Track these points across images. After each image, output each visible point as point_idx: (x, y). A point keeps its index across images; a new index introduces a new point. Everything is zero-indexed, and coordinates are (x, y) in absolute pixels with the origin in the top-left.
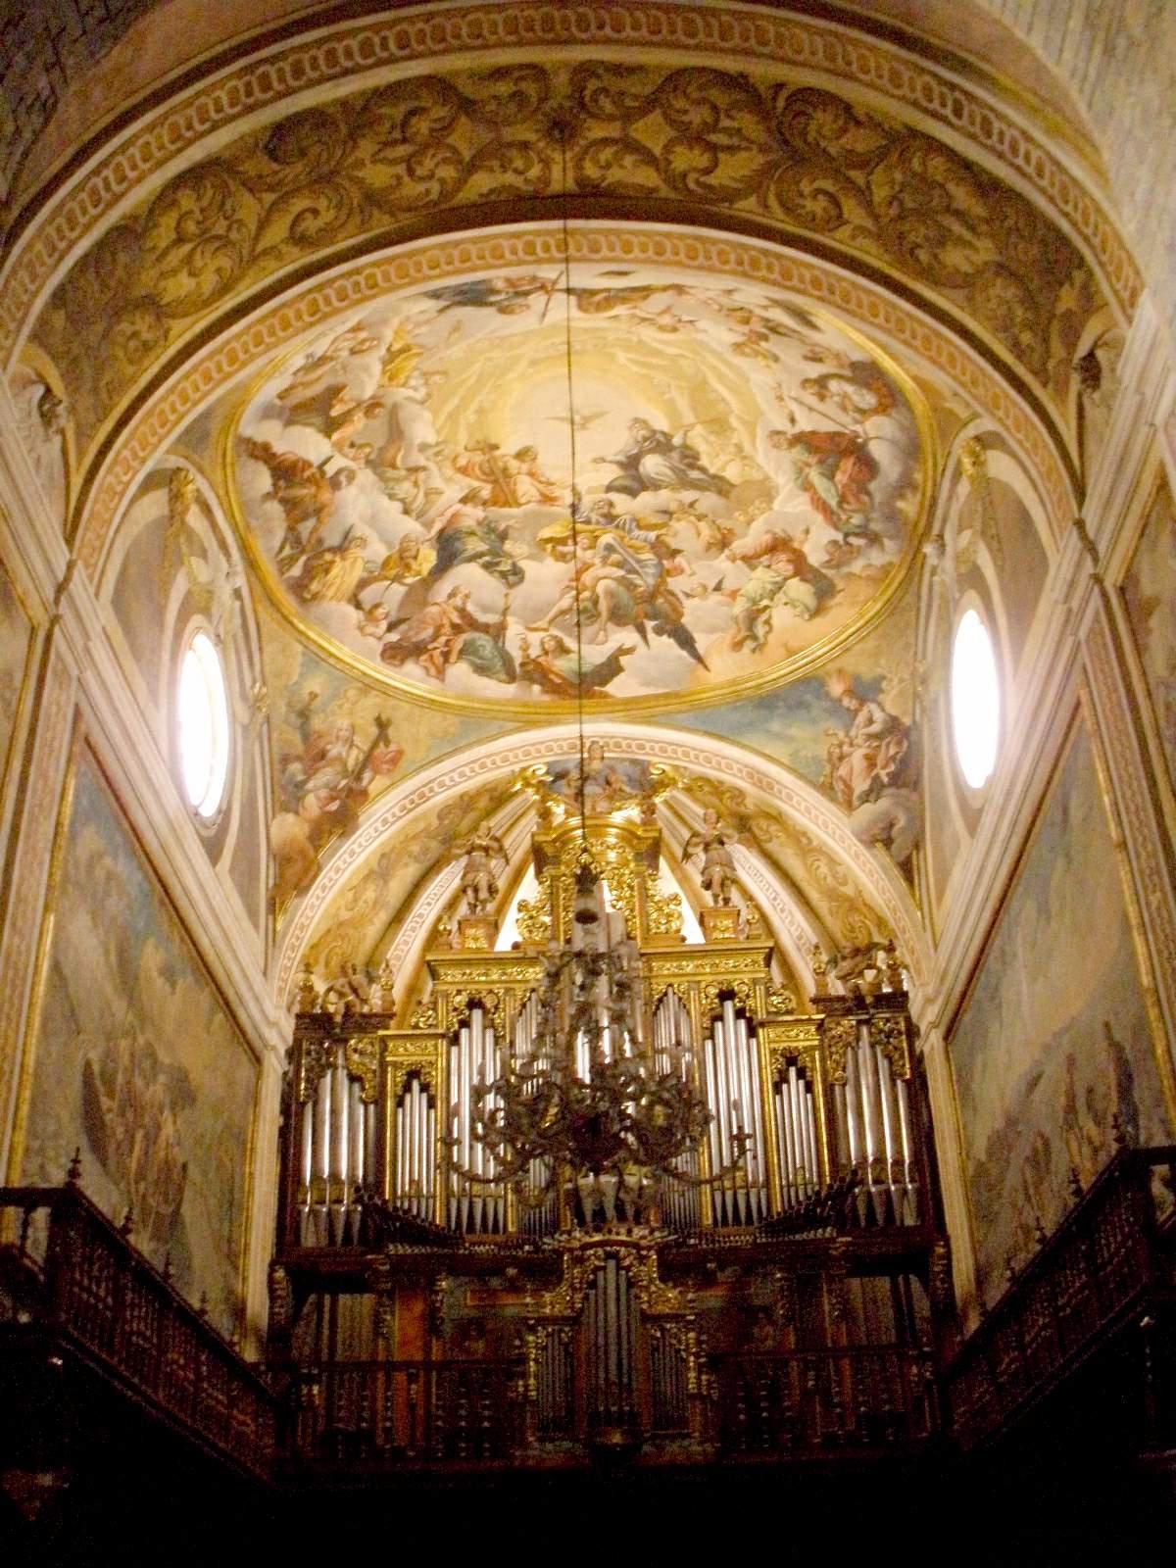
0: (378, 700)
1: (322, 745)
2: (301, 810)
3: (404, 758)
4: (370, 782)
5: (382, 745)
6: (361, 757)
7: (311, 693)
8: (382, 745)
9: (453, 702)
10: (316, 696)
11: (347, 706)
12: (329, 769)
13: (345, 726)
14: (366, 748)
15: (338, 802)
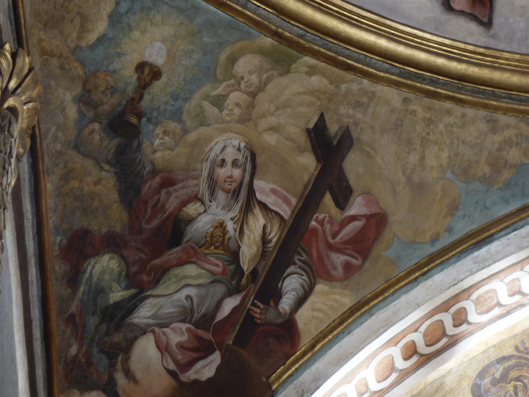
0: (316, 81)
1: (172, 204)
2: (121, 380)
3: (387, 234)
4: (300, 302)
5: (328, 199)
6: (274, 235)
7: (141, 67)
8: (328, 199)
9: (515, 79)
10: (156, 74)
11: (235, 97)
12: (191, 270)
13: (230, 154)
14: (286, 211)
15: (216, 358)
